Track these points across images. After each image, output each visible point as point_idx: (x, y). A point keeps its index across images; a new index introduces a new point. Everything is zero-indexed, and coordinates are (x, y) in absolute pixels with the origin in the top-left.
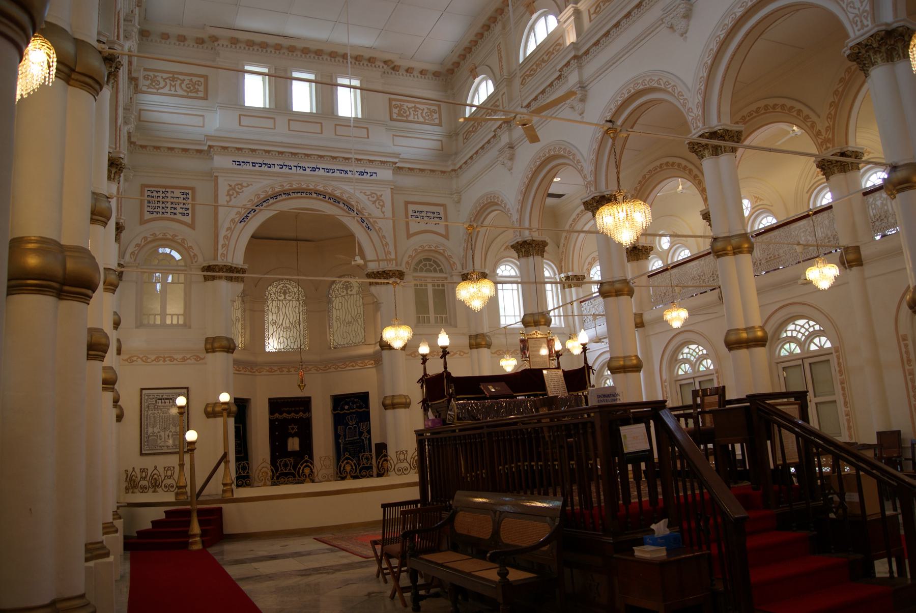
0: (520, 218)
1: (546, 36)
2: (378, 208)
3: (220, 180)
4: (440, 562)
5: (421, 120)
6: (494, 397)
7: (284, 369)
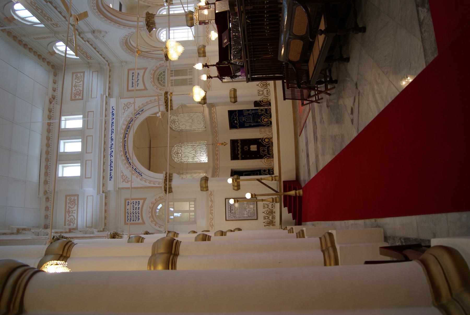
0: (133, 27)
1: (27, 11)
2: (131, 105)
3: (120, 186)
4: (313, 68)
5: (81, 83)
6: (230, 40)
7: (216, 153)
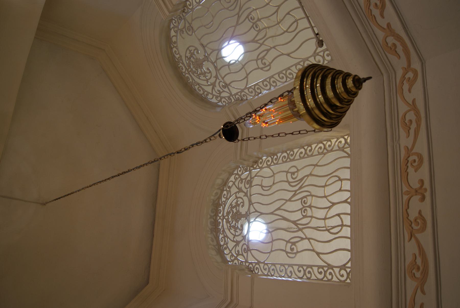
7: (413, 214)
